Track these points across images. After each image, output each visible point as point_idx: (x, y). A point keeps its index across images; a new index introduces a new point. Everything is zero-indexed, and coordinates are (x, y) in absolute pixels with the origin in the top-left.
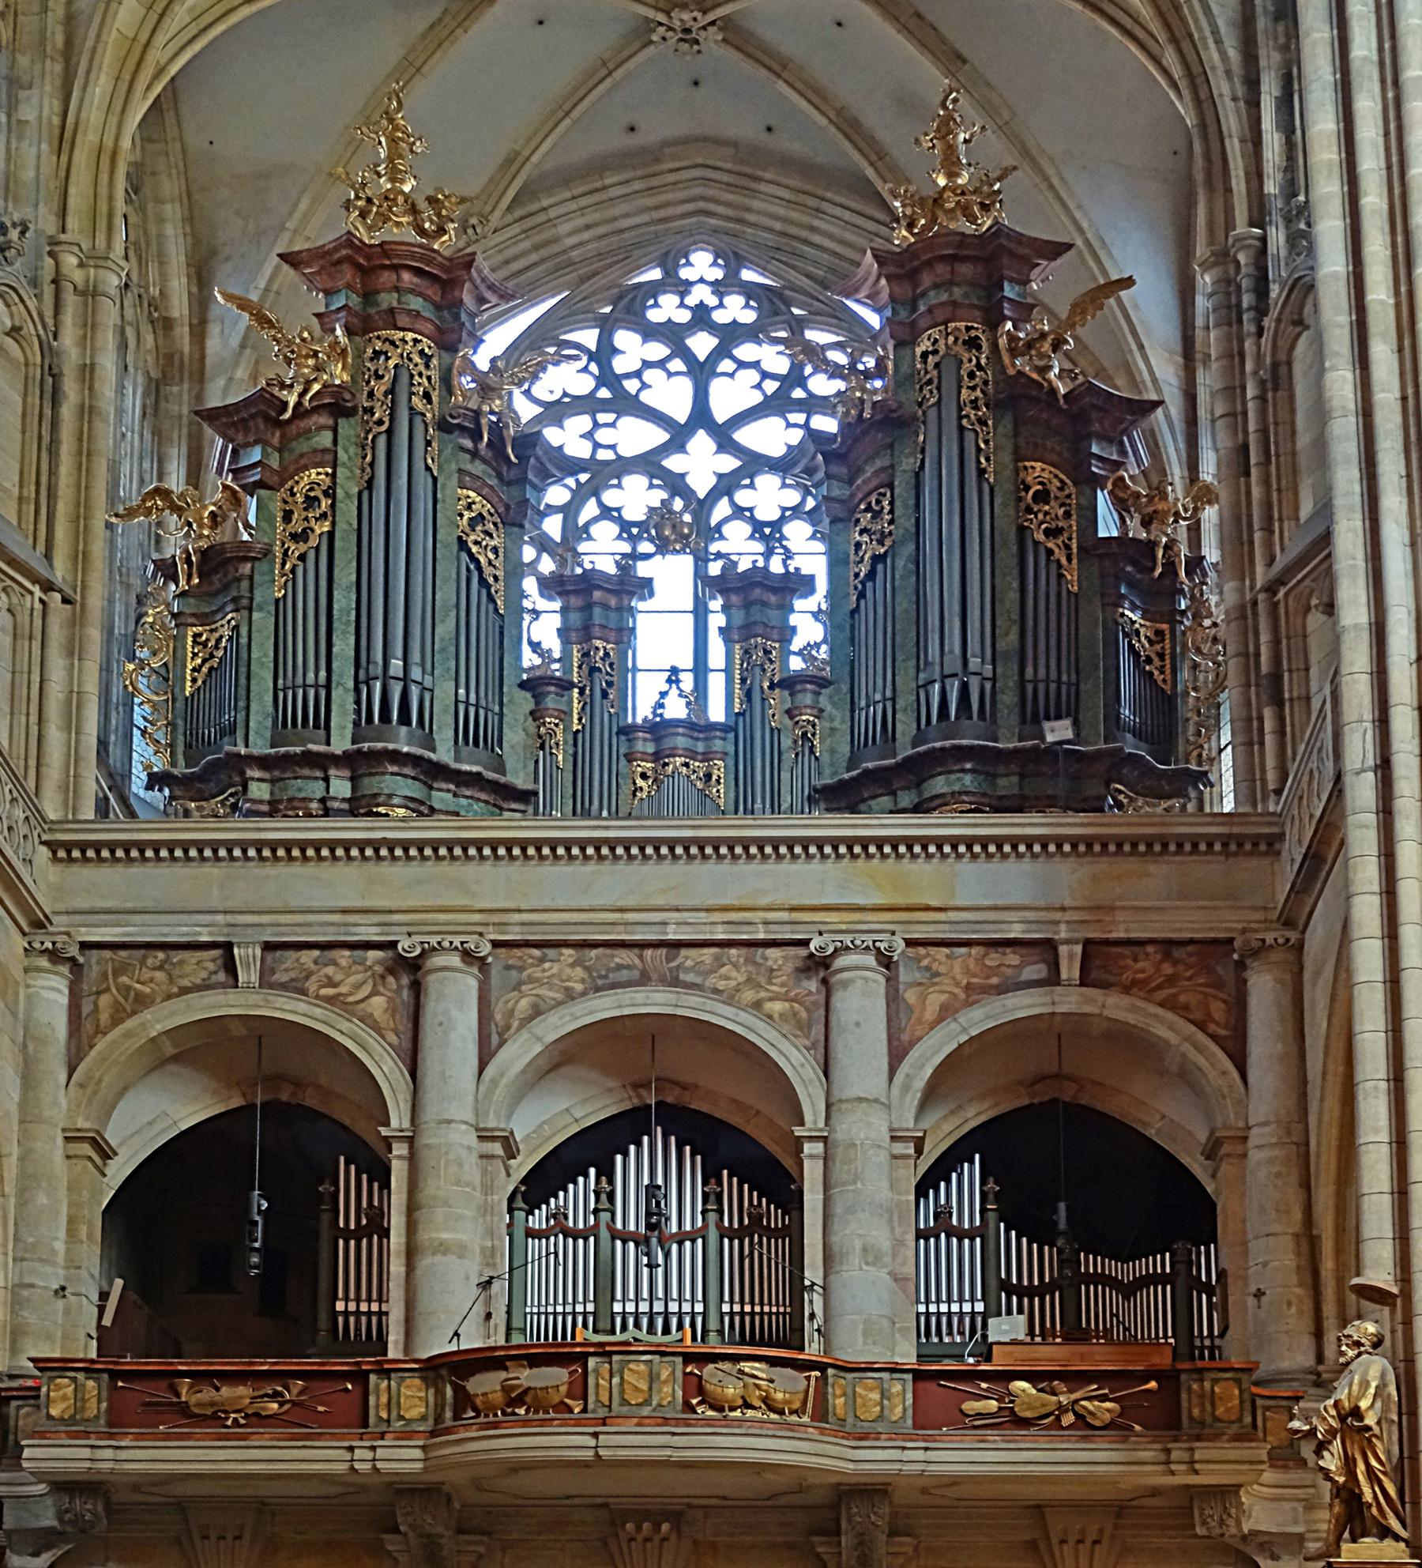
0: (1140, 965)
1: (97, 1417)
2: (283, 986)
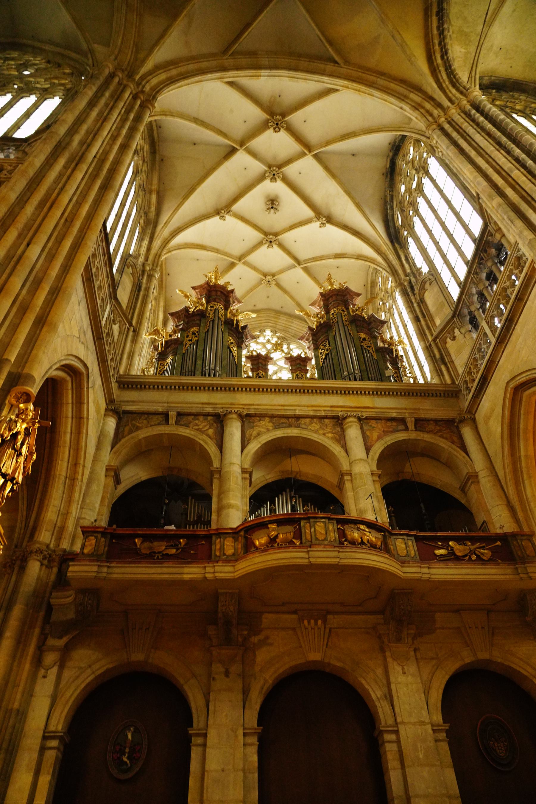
0: (430, 426)
1: (102, 554)
2: (183, 425)
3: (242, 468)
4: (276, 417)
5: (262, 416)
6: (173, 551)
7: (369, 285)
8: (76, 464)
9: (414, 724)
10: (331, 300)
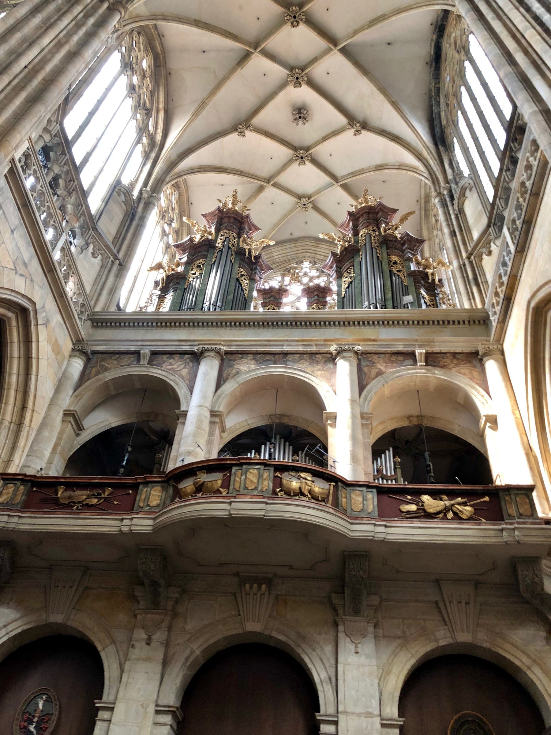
1: (18, 503)
3: (211, 411)
4: (260, 354)
5: (244, 354)
6: (95, 501)
7: (423, 201)
8: (24, 408)
9: (359, 715)
10: (361, 220)
